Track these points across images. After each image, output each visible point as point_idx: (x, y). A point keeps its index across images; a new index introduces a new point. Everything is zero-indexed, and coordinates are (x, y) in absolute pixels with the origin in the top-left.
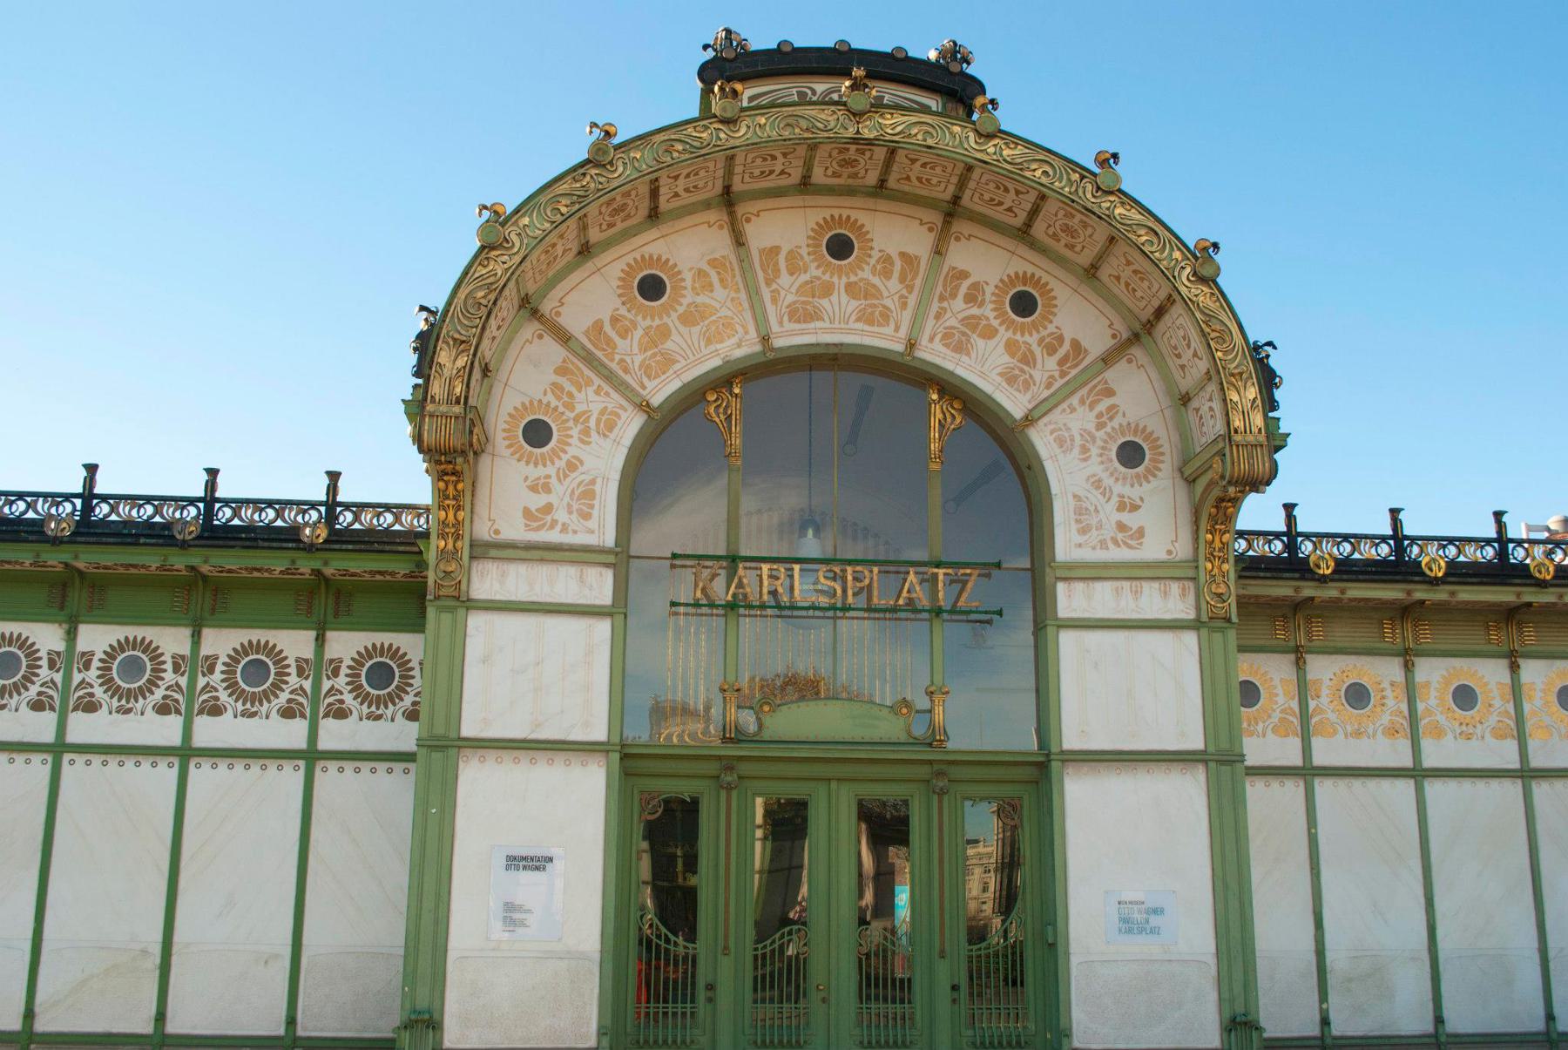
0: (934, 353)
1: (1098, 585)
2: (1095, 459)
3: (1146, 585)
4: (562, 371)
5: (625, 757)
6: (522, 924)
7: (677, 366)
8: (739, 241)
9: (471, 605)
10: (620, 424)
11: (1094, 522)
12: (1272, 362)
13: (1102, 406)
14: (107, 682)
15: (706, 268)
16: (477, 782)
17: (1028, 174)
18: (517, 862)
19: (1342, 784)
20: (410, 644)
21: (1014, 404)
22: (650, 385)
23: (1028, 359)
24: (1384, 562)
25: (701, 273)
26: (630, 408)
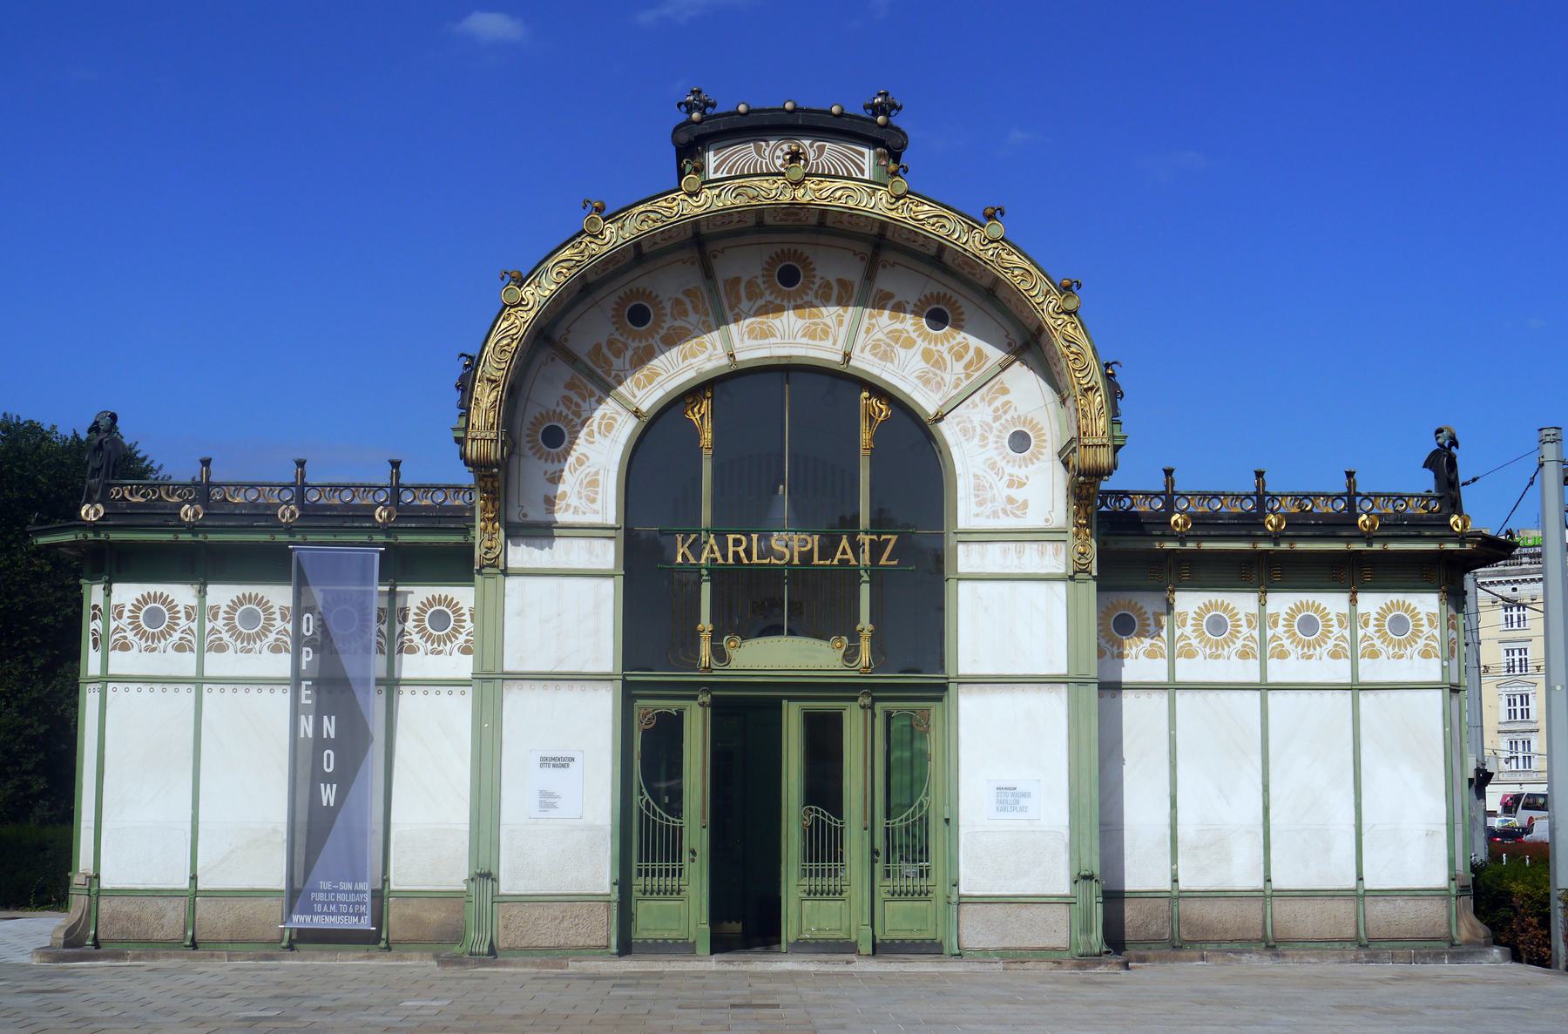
0: (865, 363)
1: (990, 546)
2: (992, 445)
3: (1027, 545)
4: (570, 386)
5: (627, 686)
6: (553, 806)
7: (660, 378)
8: (708, 274)
9: (505, 573)
10: (616, 426)
11: (989, 495)
12: (1117, 379)
13: (998, 403)
14: (232, 629)
15: (681, 296)
16: (518, 703)
17: (928, 228)
18: (546, 762)
19: (1198, 696)
20: (463, 596)
21: (927, 401)
22: (639, 394)
23: (939, 364)
24: (1248, 514)
25: (678, 302)
26: (624, 413)
